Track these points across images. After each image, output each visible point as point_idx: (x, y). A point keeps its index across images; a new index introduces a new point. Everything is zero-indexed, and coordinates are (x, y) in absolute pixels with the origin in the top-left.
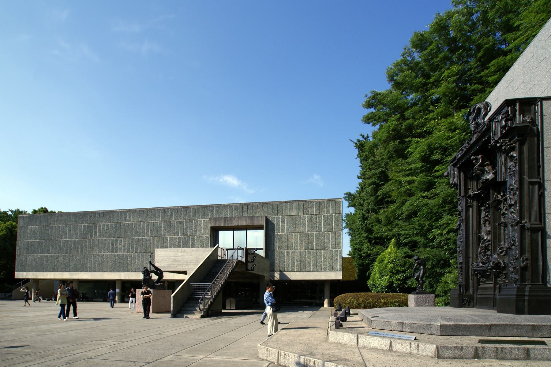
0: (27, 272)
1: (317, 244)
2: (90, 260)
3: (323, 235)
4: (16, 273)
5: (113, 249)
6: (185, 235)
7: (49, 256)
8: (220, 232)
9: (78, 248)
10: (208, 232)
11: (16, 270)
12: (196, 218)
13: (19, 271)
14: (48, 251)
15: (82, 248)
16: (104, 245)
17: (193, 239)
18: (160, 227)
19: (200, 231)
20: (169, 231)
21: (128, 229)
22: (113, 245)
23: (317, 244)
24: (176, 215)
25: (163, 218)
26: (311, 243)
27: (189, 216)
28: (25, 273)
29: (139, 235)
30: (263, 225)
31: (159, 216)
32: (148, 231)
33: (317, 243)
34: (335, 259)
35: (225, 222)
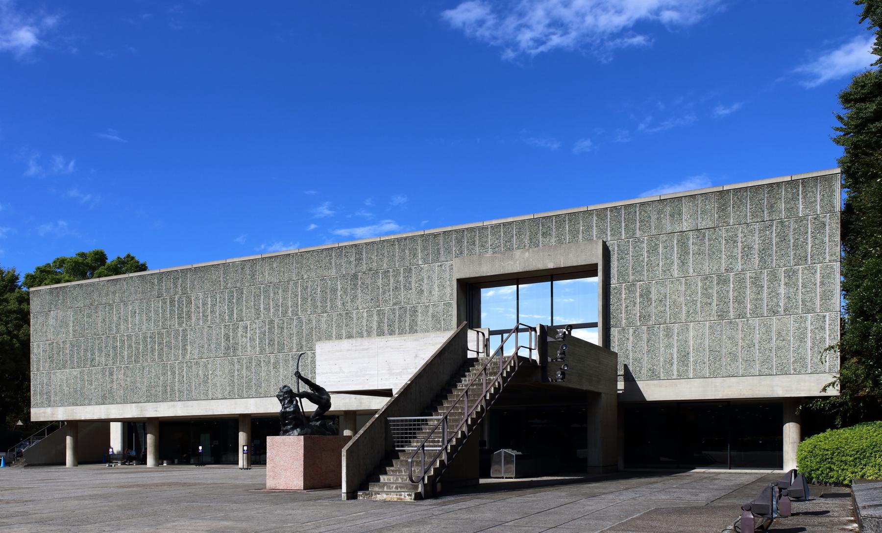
0: (53, 406)
1: (757, 300)
2: (179, 374)
3: (774, 277)
4: (33, 411)
5: (228, 348)
6: (395, 304)
7: (94, 372)
8: (481, 289)
9: (153, 351)
10: (451, 292)
11: (32, 404)
12: (420, 263)
13: (37, 406)
15: (162, 349)
16: (209, 340)
18: (334, 290)
19: (430, 292)
20: (354, 298)
21: (260, 299)
22: (227, 338)
23: (757, 300)
25: (339, 266)
28: (49, 410)
29: (286, 313)
30: (596, 265)
31: (331, 264)
32: (304, 299)
33: (756, 300)
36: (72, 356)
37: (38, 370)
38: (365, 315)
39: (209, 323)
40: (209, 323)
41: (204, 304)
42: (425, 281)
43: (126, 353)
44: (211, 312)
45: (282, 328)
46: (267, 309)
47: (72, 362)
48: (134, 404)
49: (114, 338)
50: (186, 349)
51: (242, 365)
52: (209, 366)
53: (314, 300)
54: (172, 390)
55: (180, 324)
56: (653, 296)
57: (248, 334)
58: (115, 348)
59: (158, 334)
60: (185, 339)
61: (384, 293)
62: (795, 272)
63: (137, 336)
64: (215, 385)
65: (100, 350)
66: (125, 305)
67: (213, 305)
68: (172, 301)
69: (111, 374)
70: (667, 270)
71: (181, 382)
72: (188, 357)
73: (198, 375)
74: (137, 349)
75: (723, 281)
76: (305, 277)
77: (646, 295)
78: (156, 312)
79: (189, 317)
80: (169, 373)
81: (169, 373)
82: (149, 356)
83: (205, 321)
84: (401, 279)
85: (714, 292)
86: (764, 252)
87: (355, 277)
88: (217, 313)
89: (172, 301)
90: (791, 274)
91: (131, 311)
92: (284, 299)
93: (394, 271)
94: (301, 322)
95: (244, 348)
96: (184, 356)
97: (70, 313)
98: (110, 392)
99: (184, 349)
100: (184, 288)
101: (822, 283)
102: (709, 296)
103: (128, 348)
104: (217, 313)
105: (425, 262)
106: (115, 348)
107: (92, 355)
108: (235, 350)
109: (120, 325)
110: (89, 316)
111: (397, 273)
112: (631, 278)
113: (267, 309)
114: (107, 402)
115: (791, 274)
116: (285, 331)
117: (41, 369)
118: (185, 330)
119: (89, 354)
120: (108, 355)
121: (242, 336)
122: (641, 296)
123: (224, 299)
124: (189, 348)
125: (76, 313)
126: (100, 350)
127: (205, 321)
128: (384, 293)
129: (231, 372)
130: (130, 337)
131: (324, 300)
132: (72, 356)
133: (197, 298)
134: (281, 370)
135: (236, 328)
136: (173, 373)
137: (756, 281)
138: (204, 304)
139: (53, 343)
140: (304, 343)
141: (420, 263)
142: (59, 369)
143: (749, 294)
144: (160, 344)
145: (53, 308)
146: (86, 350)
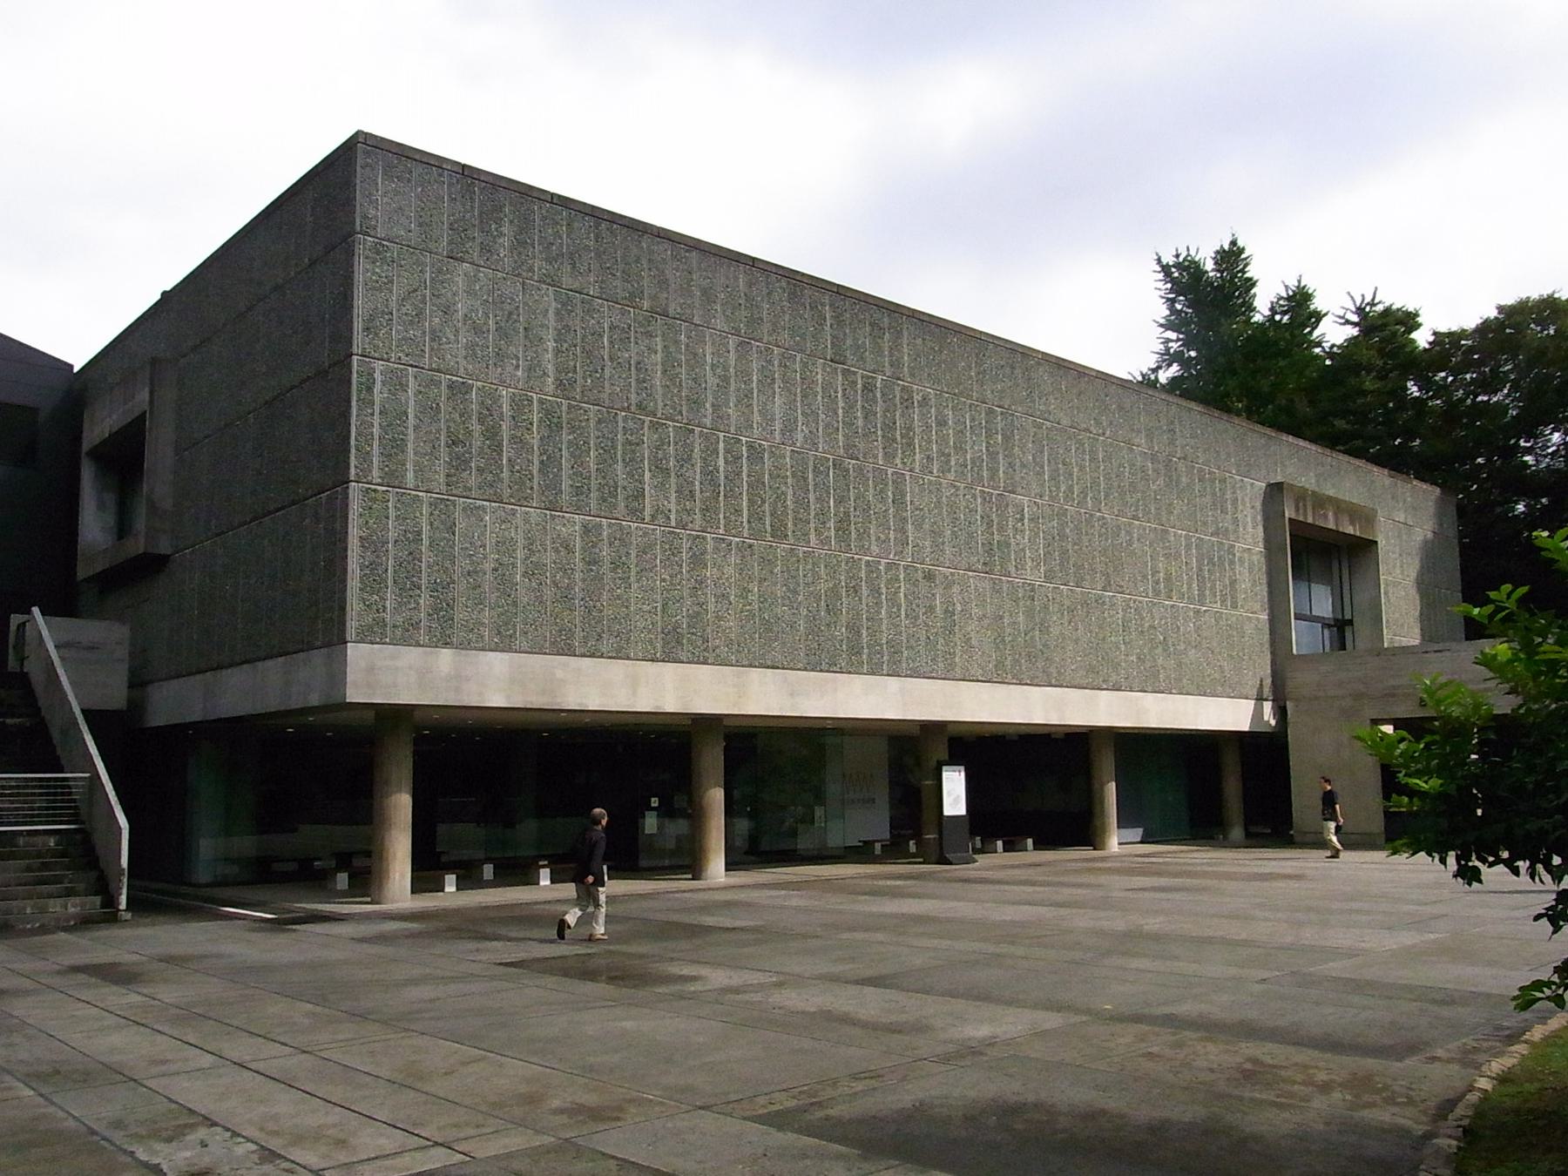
9: (822, 513)
37: (393, 479)
47: (553, 486)
55: (889, 457)
58: (710, 474)
60: (899, 501)
69: (698, 561)
82: (812, 525)
99: (904, 531)
106: (710, 474)
110: (622, 337)
118: (899, 480)
120: (686, 493)
125: (565, 305)
126: (659, 468)
130: (755, 454)
144: (840, 501)
146: (608, 453)
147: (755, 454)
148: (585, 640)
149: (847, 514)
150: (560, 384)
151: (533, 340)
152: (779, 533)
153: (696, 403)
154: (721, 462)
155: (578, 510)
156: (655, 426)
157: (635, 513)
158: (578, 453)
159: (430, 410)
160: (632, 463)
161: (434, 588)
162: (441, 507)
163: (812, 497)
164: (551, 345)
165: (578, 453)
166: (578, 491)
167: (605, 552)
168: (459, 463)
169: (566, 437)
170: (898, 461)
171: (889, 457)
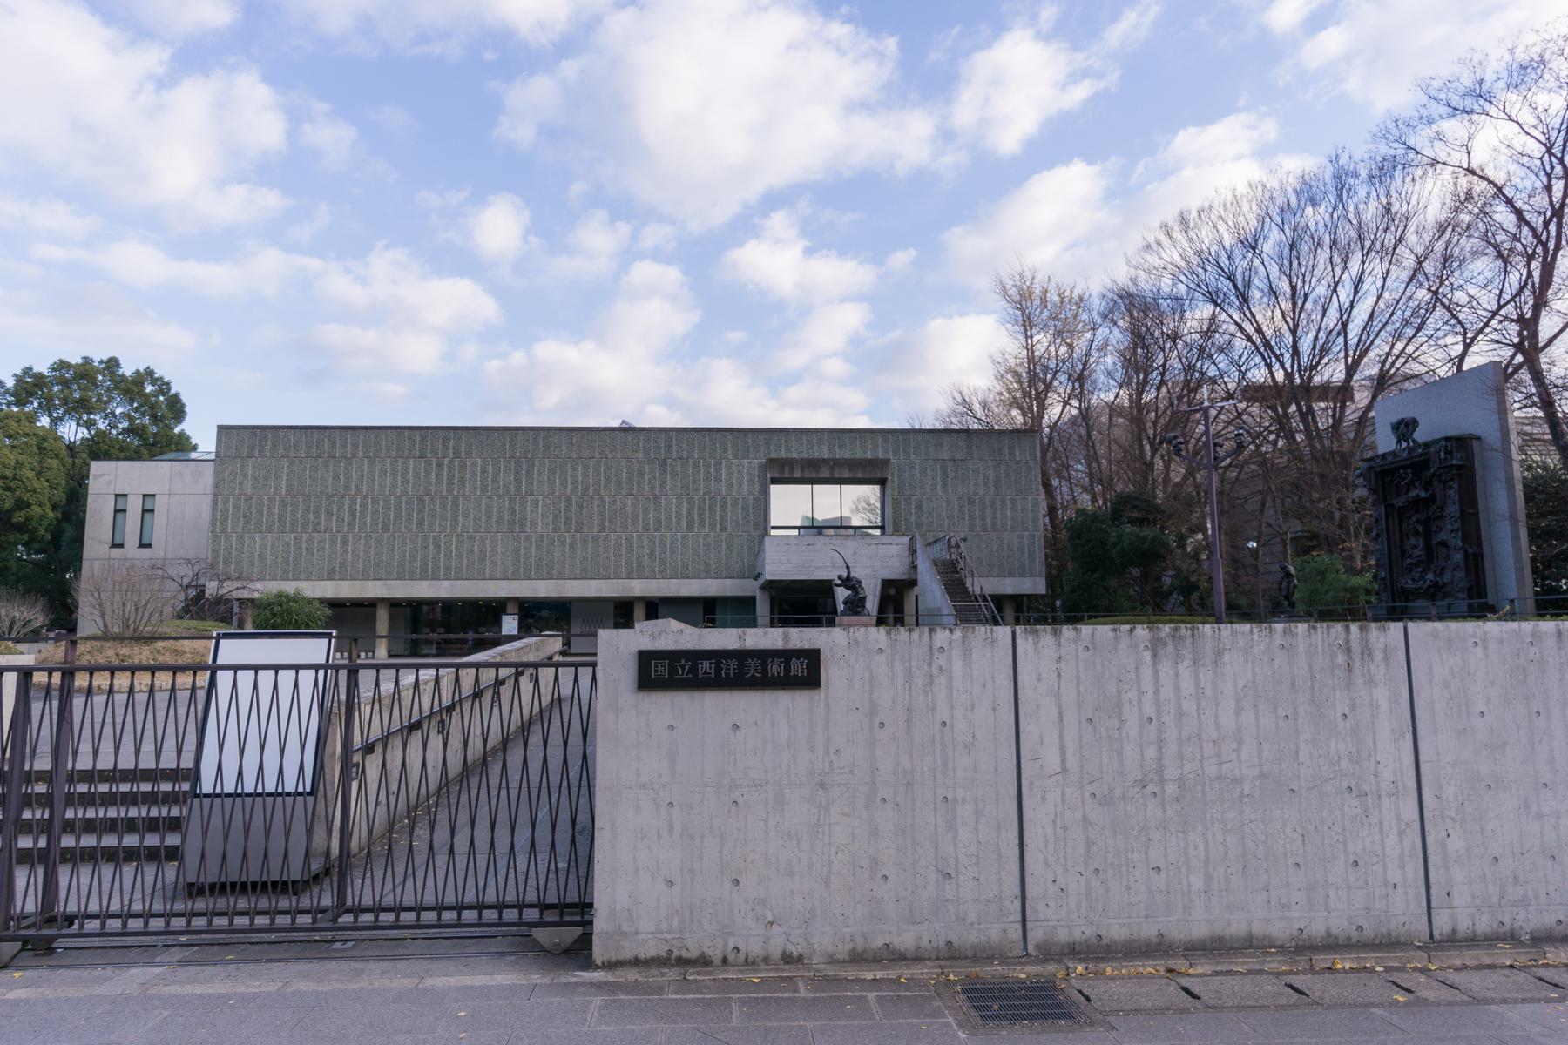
3: (1003, 503)
5: (512, 523)
9: (409, 519)
14: (319, 523)
17: (724, 503)
18: (642, 473)
21: (555, 473)
24: (681, 447)
25: (647, 451)
26: (983, 518)
27: (714, 451)
32: (608, 479)
34: (1029, 551)
35: (802, 470)
36: (282, 518)
38: (674, 501)
39: (489, 493)
40: (489, 493)
41: (484, 471)
42: (736, 475)
43: (369, 520)
44: (493, 481)
45: (582, 507)
46: (564, 485)
47: (283, 524)
48: (378, 582)
49: (350, 498)
50: (456, 520)
51: (531, 543)
52: (488, 542)
53: (619, 484)
54: (436, 566)
55: (450, 492)
56: (925, 508)
57: (540, 510)
58: (352, 512)
59: (419, 499)
61: (694, 482)
62: (1016, 501)
63: (386, 501)
64: (494, 563)
65: (329, 513)
66: (372, 462)
67: (496, 475)
68: (440, 465)
69: (345, 543)
70: (934, 488)
71: (448, 557)
72: (459, 530)
73: (472, 551)
74: (387, 515)
75: (971, 502)
76: (610, 456)
77: (919, 506)
78: (417, 476)
79: (462, 482)
80: (431, 547)
81: (431, 547)
83: (485, 490)
84: (712, 470)
85: (966, 509)
86: (997, 482)
87: (664, 462)
88: (501, 484)
89: (440, 465)
90: (1013, 502)
91: (381, 470)
92: (586, 475)
93: (704, 462)
94: (603, 501)
95: (534, 524)
96: (453, 527)
97: (285, 463)
98: (343, 565)
100: (457, 454)
101: (1033, 511)
102: (963, 513)
103: (372, 513)
104: (501, 484)
105: (736, 457)
106: (352, 512)
107: (316, 518)
108: (522, 525)
109: (362, 484)
111: (707, 466)
112: (909, 492)
113: (564, 485)
114: (337, 577)
115: (1013, 502)
116: (585, 509)
117: (229, 530)
119: (311, 516)
120: (340, 519)
121: (532, 511)
122: (916, 507)
123: (510, 469)
124: (460, 518)
126: (329, 513)
127: (485, 490)
128: (694, 482)
129: (517, 551)
130: (375, 501)
131: (630, 480)
132: (282, 518)
133: (475, 464)
134: (579, 551)
135: (523, 503)
136: (437, 546)
137: (993, 504)
138: (484, 471)
139: (251, 498)
140: (607, 524)
141: (730, 457)
142: (261, 532)
143: (988, 512)
144: (420, 512)
145: (256, 455)
147: (375, 501)
148: (293, 575)
149: (423, 518)
150: (287, 491)
151: (277, 477)
152: (385, 529)
153: (347, 488)
154: (358, 506)
155: (292, 532)
156: (327, 499)
157: (316, 530)
158: (294, 513)
159: (237, 507)
160: (317, 511)
161: (236, 562)
162: (241, 537)
163: (404, 514)
164: (285, 478)
165: (294, 513)
166: (293, 526)
167: (304, 545)
168: (248, 522)
169: (289, 508)
170: (455, 493)
171: (450, 492)
